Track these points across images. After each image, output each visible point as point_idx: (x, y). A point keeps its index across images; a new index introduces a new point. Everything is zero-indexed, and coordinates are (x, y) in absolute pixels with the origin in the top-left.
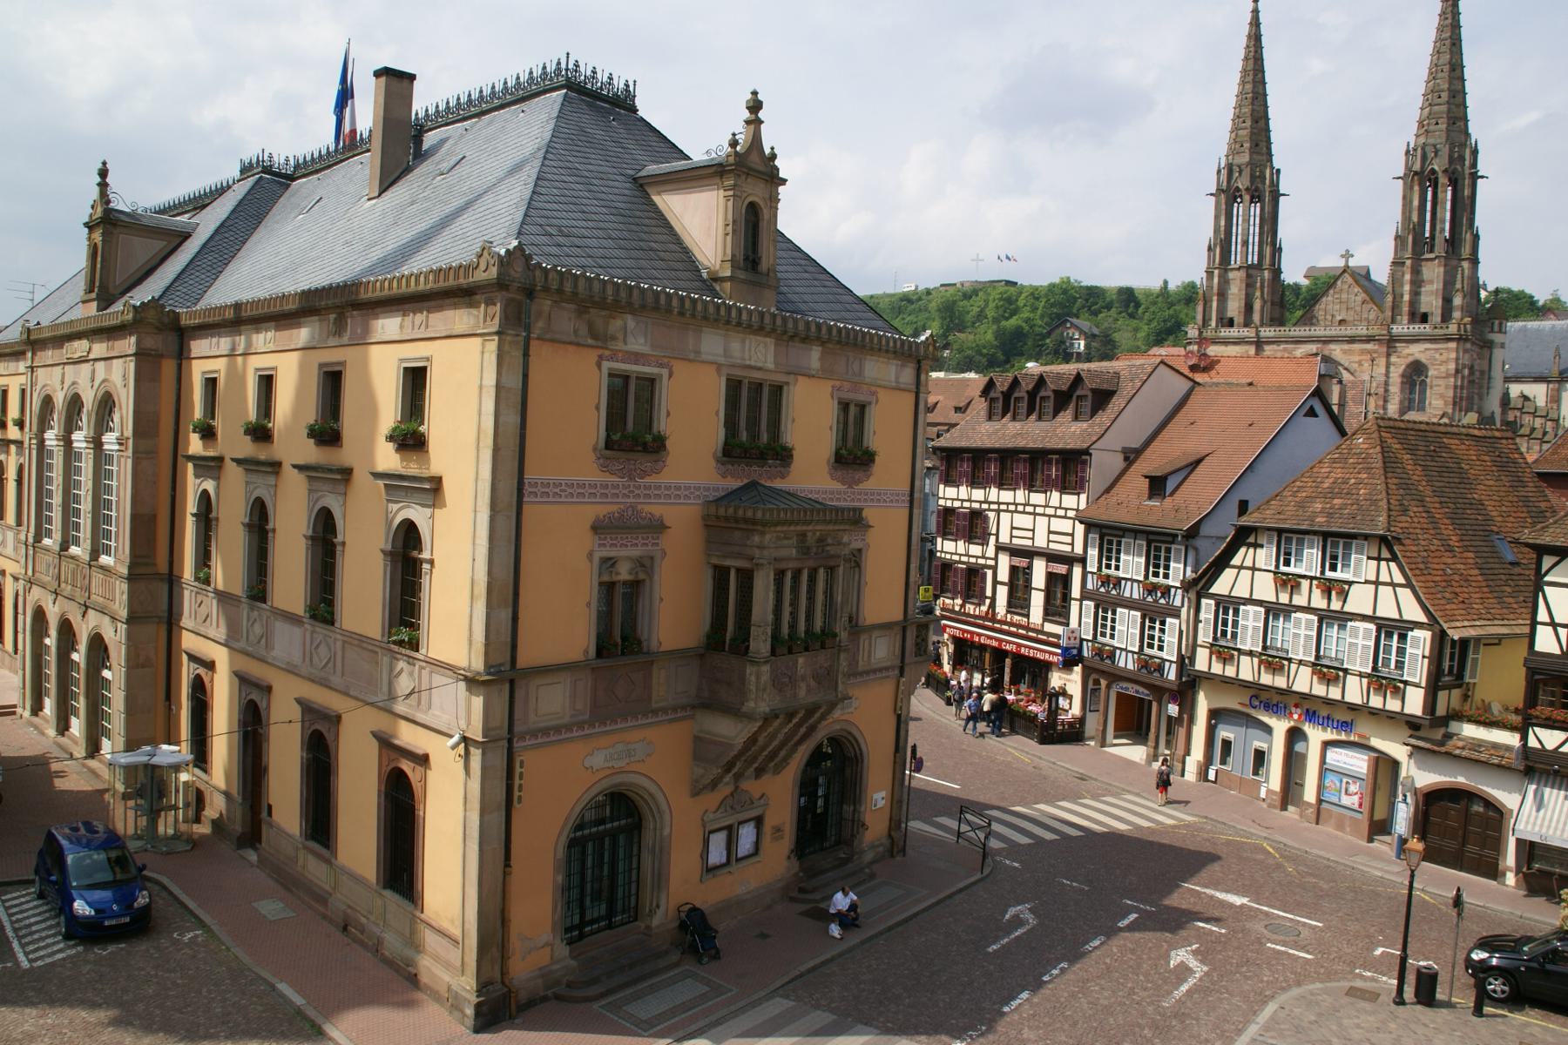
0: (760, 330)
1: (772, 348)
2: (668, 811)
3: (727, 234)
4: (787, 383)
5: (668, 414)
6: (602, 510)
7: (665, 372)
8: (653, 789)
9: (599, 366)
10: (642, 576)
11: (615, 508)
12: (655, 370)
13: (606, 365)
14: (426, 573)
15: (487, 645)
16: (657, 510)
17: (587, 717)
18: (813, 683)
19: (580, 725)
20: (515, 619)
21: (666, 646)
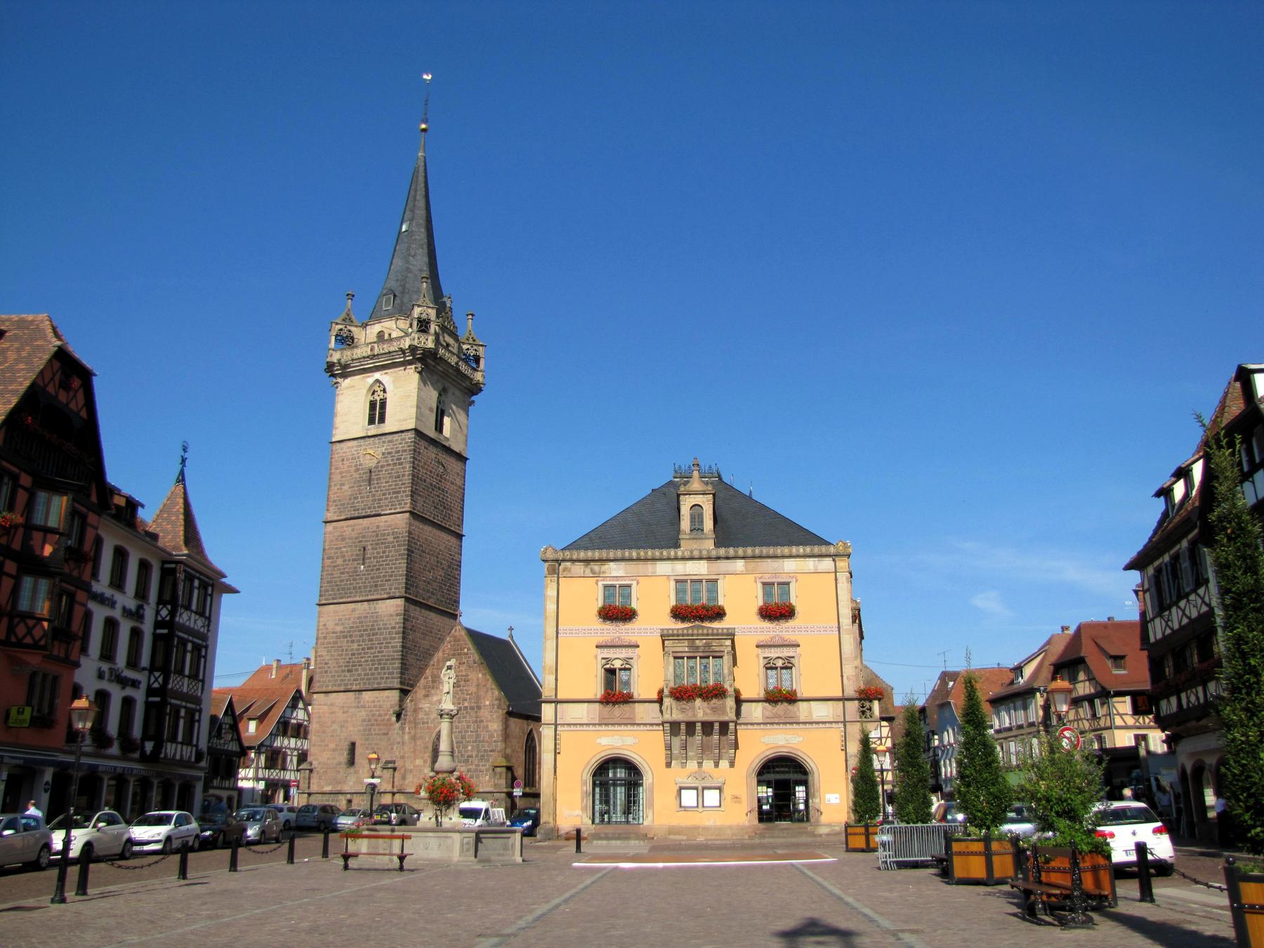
0: (701, 558)
1: (706, 565)
2: (650, 772)
5: (638, 599)
6: (601, 639)
7: (634, 583)
8: (640, 759)
9: (597, 584)
11: (607, 638)
12: (629, 582)
13: (600, 583)
16: (633, 639)
17: (597, 722)
18: (708, 711)
19: (594, 725)
20: (556, 679)
21: (643, 696)
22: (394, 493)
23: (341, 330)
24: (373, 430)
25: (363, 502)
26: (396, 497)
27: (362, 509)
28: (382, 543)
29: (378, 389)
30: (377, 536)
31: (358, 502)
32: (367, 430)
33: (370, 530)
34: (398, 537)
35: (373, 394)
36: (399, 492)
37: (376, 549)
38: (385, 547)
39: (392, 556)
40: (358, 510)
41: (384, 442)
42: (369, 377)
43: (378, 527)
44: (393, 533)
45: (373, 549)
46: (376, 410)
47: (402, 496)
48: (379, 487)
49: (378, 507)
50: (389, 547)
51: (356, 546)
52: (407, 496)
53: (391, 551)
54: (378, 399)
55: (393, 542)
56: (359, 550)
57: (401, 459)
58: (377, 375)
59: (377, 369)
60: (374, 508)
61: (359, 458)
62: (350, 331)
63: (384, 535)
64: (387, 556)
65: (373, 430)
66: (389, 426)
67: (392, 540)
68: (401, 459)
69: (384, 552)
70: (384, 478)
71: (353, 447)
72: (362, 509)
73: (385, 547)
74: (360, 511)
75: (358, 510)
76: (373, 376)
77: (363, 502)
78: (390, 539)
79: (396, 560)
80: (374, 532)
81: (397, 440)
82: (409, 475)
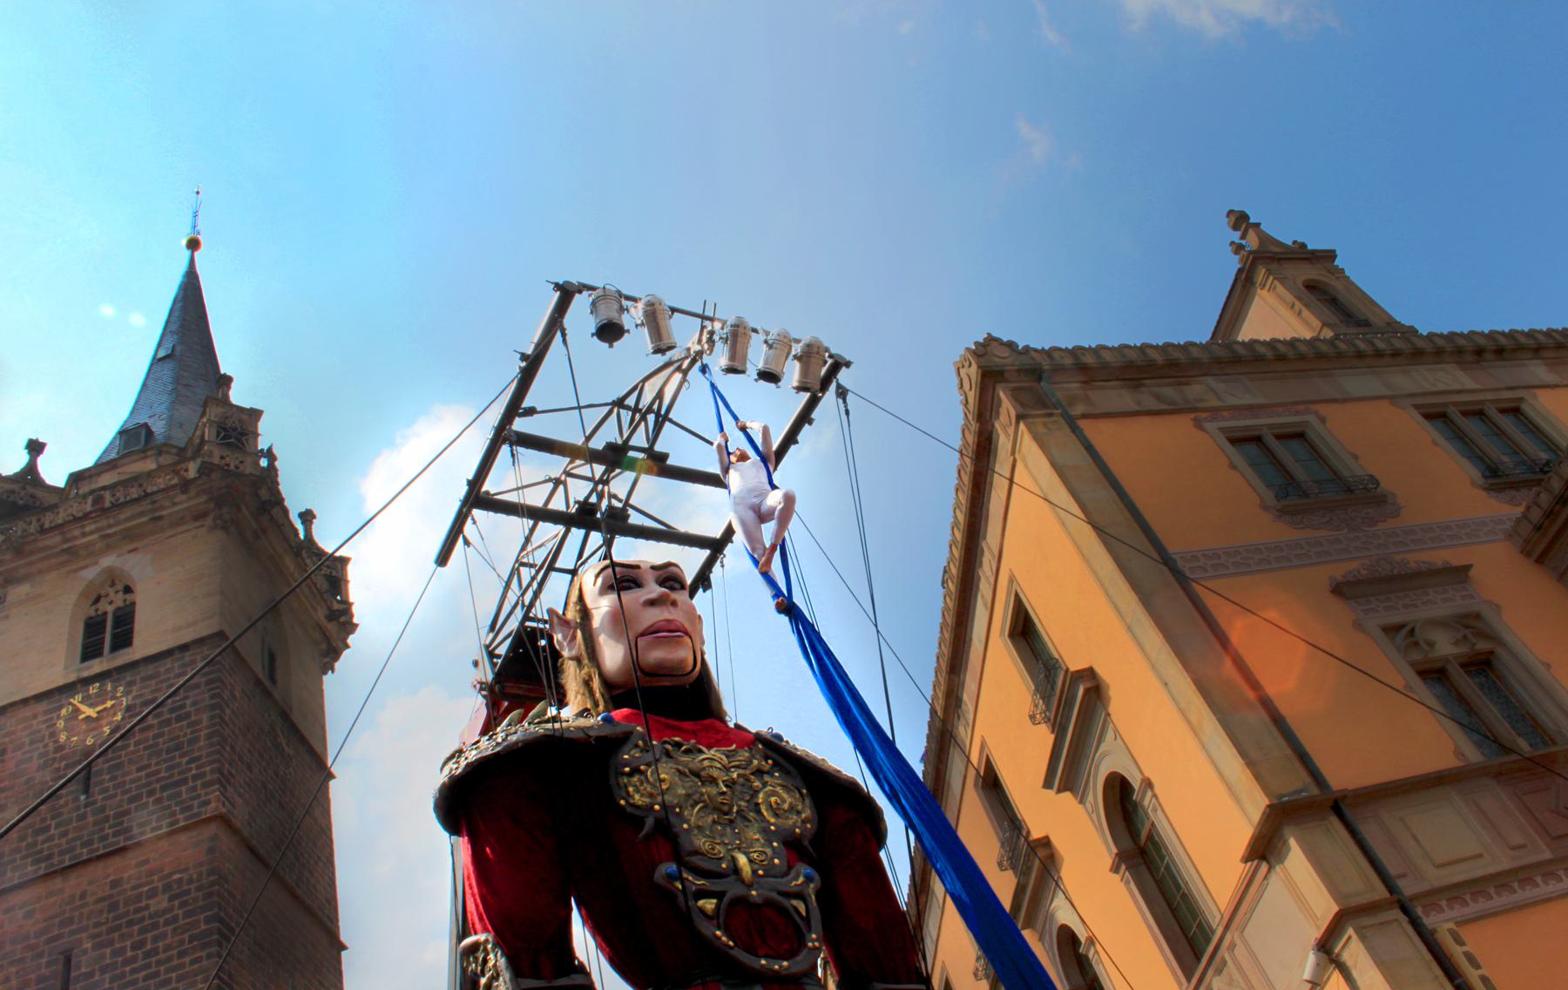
3: (1300, 313)
4: (1521, 399)
10: (1483, 646)
14: (1155, 810)
15: (1250, 764)
22: (163, 789)
23: (13, 492)
24: (97, 666)
25: (65, 834)
26: (170, 798)
27: (62, 853)
28: (131, 923)
29: (111, 591)
30: (113, 907)
31: (51, 839)
32: (80, 670)
33: (90, 899)
34: (188, 892)
35: (97, 600)
36: (185, 781)
37: (111, 943)
38: (143, 931)
39: (167, 948)
40: (50, 857)
41: (130, 684)
42: (86, 567)
43: (115, 884)
44: (168, 887)
45: (99, 946)
46: (104, 632)
47: (194, 789)
48: (115, 787)
49: (115, 834)
50: (155, 926)
51: (41, 955)
52: (211, 783)
53: (164, 936)
54: (110, 609)
55: (171, 909)
56: (49, 964)
57: (183, 707)
58: (108, 561)
59: (110, 543)
60: (105, 837)
61: (53, 735)
62: (32, 496)
63: (139, 898)
64: (148, 955)
65: (97, 666)
66: (145, 642)
67: (165, 904)
68: (183, 707)
69: (137, 946)
70: (130, 762)
71: (35, 717)
72: (62, 853)
73: (141, 931)
74: (56, 860)
75: (50, 857)
76: (96, 563)
77: (65, 834)
78: (161, 902)
79: (182, 954)
80: (103, 899)
81: (168, 671)
82: (209, 736)
